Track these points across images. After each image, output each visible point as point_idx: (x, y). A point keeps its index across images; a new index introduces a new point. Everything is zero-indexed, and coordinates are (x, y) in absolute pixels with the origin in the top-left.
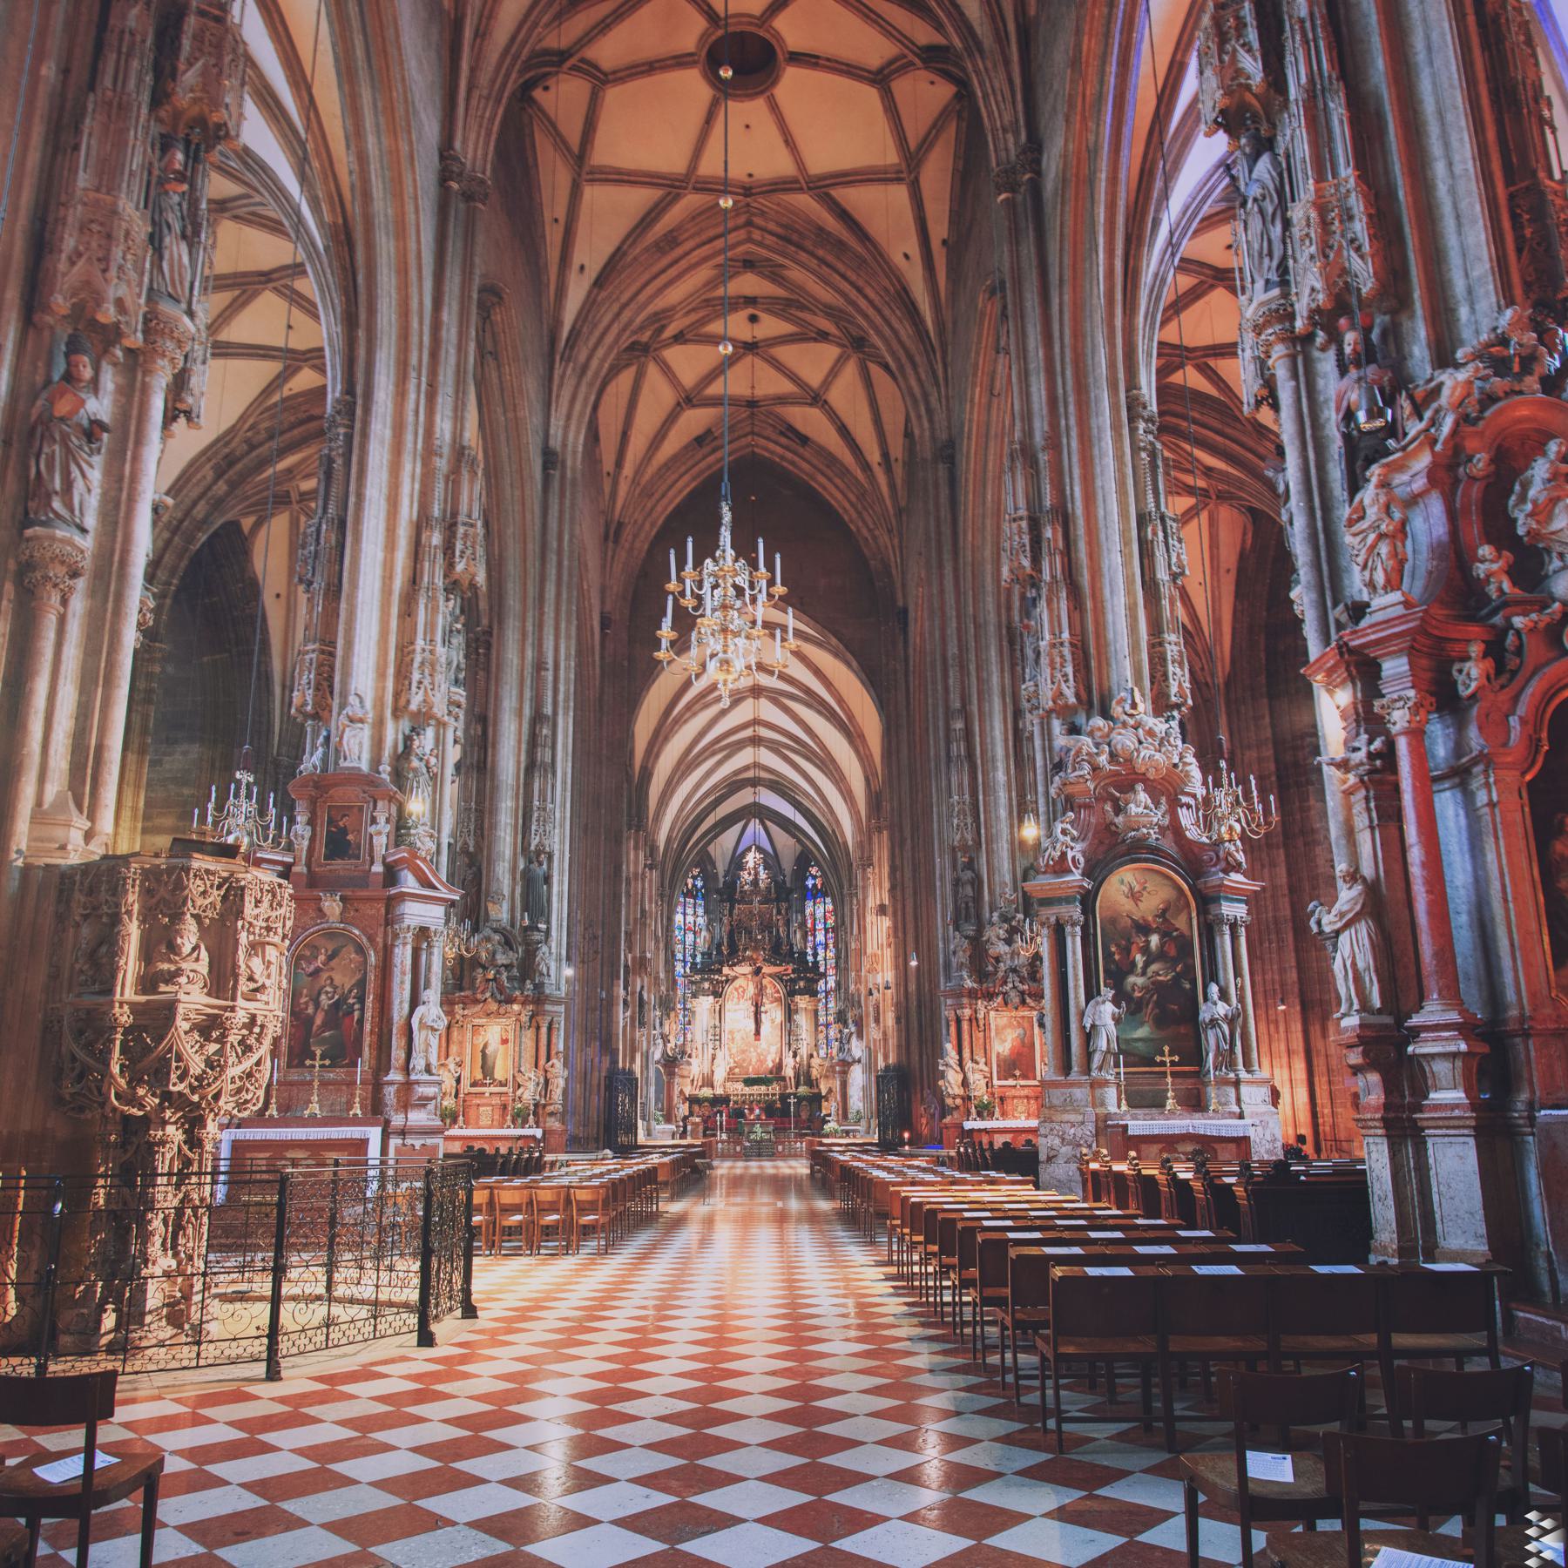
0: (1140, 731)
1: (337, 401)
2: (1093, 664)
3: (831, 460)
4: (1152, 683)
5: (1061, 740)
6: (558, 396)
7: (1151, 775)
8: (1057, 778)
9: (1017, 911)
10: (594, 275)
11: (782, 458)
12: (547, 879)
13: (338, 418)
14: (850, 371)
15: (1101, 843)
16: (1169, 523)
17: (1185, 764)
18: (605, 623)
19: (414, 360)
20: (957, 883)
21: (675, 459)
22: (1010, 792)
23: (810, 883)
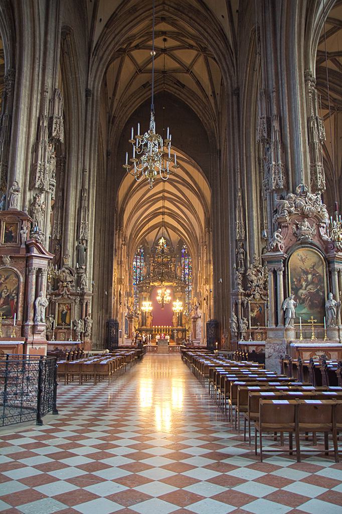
0: (306, 198)
1: (9, 71)
2: (290, 173)
3: (193, 94)
4: (311, 181)
5: (277, 200)
6: (91, 69)
8: (275, 216)
10: (105, 23)
11: (175, 93)
12: (86, 250)
13: (9, 77)
14: (201, 60)
15: (291, 240)
16: (319, 120)
17: (323, 211)
18: (108, 154)
19: (37, 56)
21: (135, 93)
22: (258, 219)
23: (183, 251)
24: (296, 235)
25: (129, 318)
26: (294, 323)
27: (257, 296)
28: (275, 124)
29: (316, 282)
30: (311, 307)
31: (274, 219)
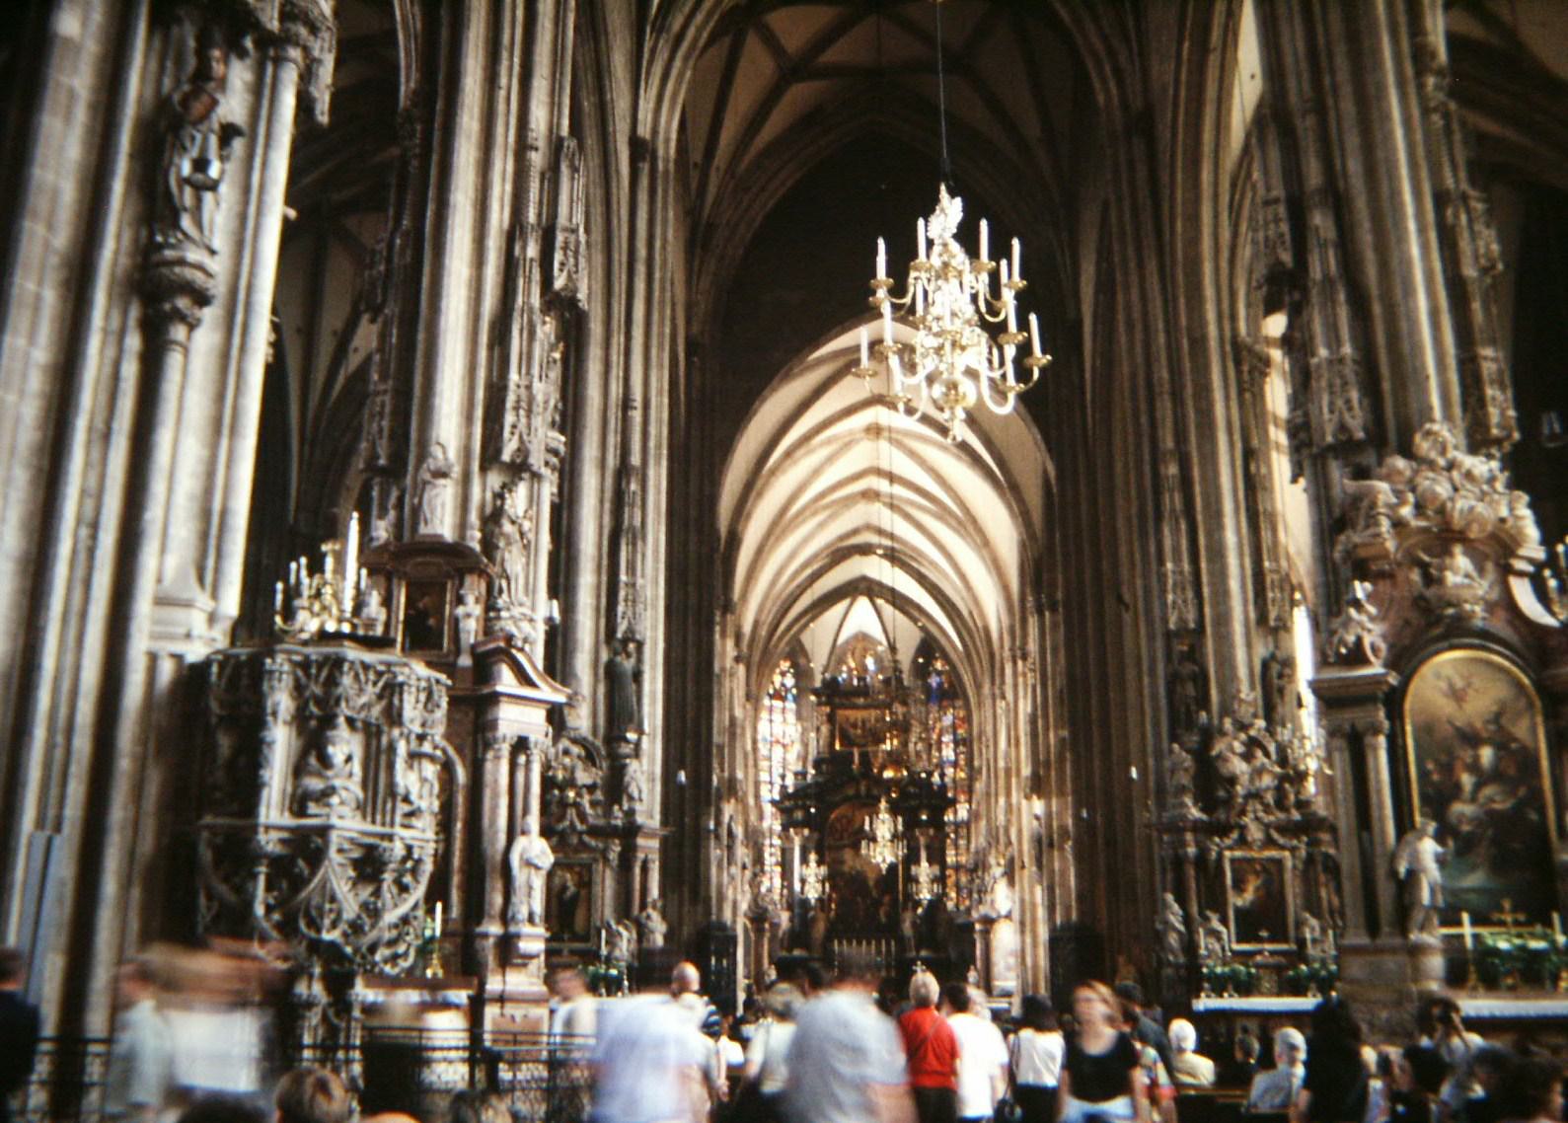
0: (1455, 474)
2: (1386, 386)
7: (1474, 533)
8: (1342, 538)
9: (1255, 716)
12: (637, 676)
15: (1407, 622)
17: (1518, 518)
20: (1173, 680)
22: (1241, 555)
23: (934, 681)
24: (1423, 604)
25: (753, 920)
26: (1444, 923)
27: (1255, 833)
28: (1321, 221)
29: (1512, 771)
30: (1499, 865)
31: (1339, 548)
